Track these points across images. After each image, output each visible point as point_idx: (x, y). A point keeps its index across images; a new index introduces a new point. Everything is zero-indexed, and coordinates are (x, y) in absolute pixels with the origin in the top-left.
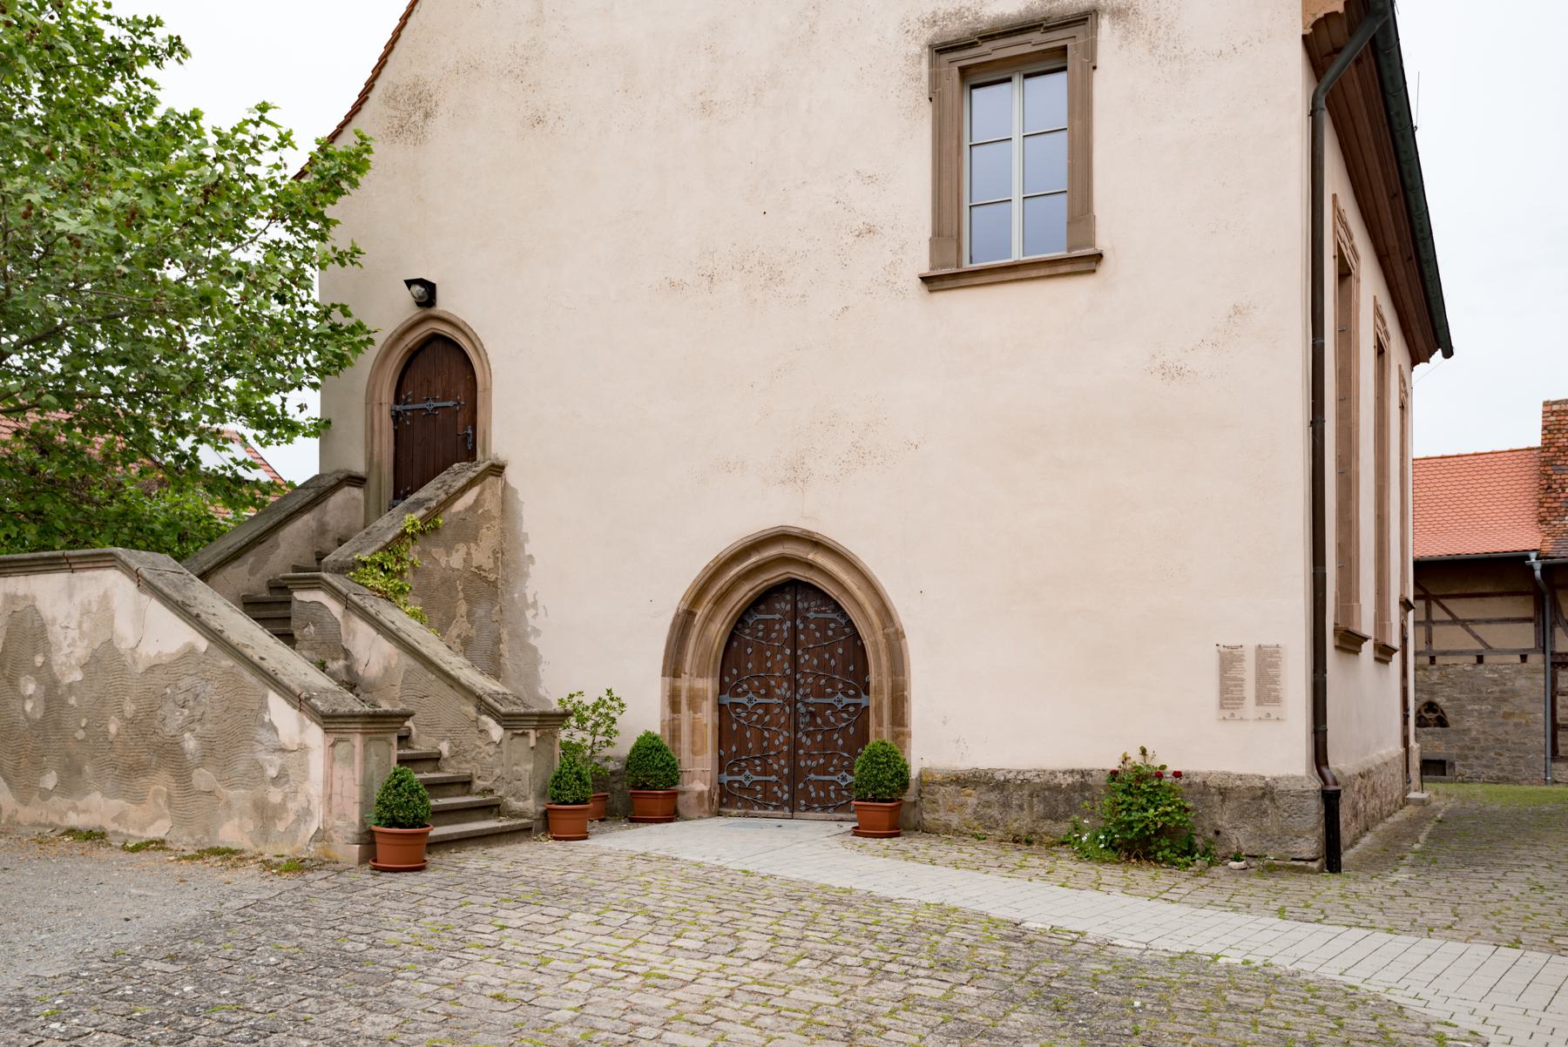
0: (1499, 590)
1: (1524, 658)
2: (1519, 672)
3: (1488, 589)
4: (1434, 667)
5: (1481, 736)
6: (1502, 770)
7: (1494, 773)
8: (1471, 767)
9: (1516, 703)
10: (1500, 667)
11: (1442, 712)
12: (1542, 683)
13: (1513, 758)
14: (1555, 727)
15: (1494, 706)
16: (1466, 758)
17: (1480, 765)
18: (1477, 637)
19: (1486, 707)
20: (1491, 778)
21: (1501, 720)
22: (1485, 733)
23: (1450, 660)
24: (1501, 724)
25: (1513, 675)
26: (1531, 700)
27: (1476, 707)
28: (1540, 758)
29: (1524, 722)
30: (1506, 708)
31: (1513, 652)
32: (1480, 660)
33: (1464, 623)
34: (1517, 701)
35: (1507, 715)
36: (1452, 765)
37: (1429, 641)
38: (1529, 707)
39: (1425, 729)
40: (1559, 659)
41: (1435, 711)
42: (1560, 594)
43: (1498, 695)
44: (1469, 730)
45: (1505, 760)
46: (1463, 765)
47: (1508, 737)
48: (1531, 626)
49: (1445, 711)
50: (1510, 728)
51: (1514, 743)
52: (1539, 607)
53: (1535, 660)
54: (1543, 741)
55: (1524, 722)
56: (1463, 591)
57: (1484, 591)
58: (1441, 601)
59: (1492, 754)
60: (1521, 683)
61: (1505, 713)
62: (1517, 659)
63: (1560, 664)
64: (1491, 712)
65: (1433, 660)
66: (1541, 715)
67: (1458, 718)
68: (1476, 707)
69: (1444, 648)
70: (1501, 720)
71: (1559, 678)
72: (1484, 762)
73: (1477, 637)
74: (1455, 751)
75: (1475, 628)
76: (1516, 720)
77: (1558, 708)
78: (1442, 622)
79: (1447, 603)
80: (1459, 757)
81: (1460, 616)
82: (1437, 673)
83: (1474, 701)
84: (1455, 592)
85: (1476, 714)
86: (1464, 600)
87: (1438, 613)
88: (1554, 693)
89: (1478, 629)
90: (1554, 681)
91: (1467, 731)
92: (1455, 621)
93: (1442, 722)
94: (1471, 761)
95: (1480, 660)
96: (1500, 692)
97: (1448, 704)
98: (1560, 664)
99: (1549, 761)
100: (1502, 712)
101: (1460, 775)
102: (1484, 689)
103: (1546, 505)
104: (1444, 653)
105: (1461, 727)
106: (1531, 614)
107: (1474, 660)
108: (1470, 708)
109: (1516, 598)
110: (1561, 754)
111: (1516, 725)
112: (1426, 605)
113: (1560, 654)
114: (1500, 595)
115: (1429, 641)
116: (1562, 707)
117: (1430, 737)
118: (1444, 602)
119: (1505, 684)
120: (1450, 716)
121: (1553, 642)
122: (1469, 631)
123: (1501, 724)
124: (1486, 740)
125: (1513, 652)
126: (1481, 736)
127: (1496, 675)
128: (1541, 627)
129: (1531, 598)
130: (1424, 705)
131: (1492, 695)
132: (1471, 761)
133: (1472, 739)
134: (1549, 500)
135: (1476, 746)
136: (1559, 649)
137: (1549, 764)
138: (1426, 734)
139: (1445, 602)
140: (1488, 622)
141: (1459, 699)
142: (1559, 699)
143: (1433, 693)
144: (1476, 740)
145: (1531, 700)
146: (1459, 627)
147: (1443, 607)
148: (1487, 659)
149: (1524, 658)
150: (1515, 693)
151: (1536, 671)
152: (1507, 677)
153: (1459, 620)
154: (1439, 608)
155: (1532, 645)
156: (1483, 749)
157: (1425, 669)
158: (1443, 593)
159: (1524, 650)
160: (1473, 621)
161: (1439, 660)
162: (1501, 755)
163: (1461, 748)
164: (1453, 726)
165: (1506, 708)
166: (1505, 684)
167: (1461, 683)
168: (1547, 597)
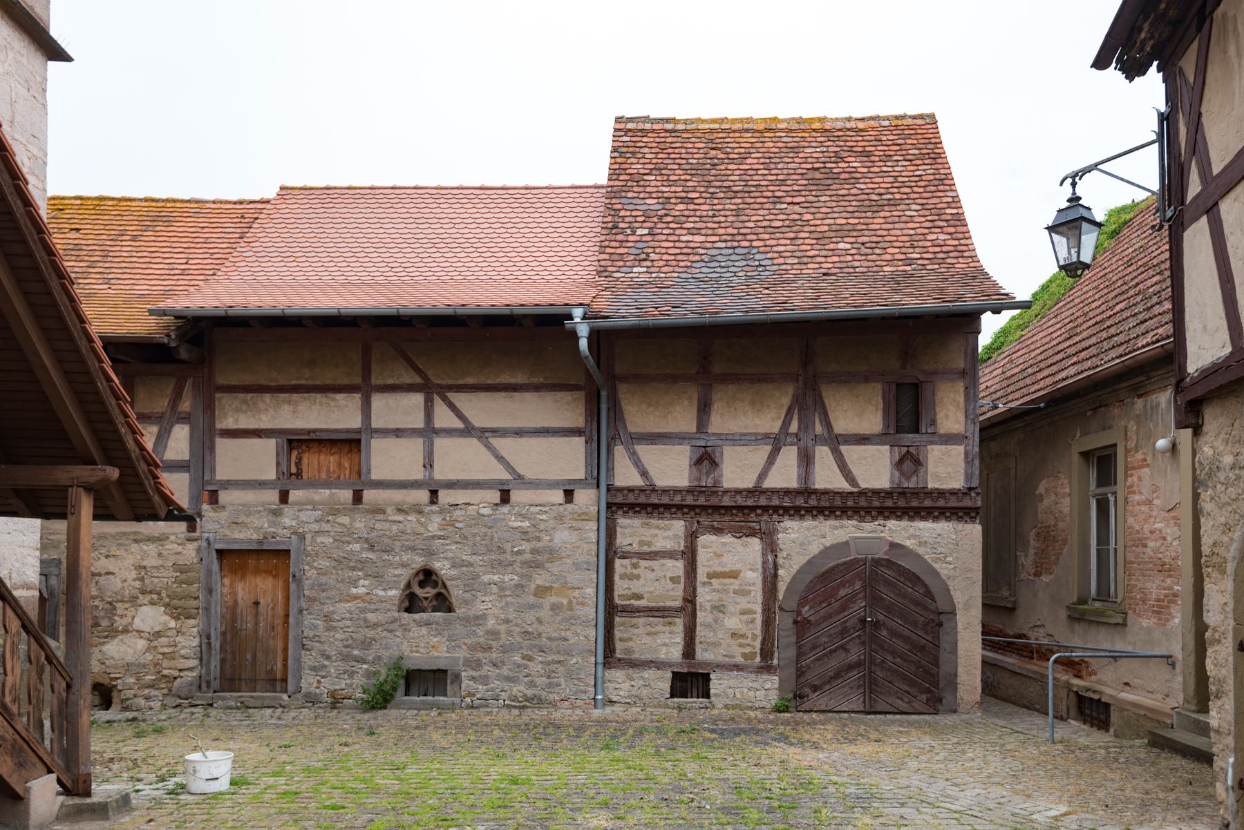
0: (535, 380)
1: (569, 495)
2: (560, 518)
3: (519, 379)
4: (435, 508)
5: (503, 628)
6: (532, 684)
7: (519, 689)
8: (485, 680)
9: (555, 570)
10: (533, 509)
11: (445, 586)
12: (593, 537)
13: (548, 663)
14: (611, 610)
15: (522, 576)
16: (478, 665)
17: (498, 677)
18: (500, 459)
19: (510, 578)
20: (515, 699)
21: (532, 599)
22: (507, 621)
23: (460, 496)
24: (532, 607)
25: (551, 523)
26: (577, 566)
27: (496, 578)
28: (586, 664)
29: (565, 601)
30: (540, 579)
31: (552, 485)
32: (505, 498)
33: (484, 434)
34: (555, 568)
35: (541, 591)
36: (457, 677)
37: (429, 464)
38: (574, 578)
39: (417, 616)
40: (619, 499)
41: (435, 584)
42: (622, 389)
43: (528, 556)
44: (484, 617)
45: (535, 667)
46: (473, 678)
47: (541, 628)
48: (579, 442)
49: (448, 583)
50: (545, 613)
51: (549, 639)
52: (593, 413)
53: (586, 498)
54: (588, 635)
55: (565, 601)
56: (483, 380)
57: (512, 381)
58: (449, 395)
59: (517, 658)
60: (562, 536)
61: (538, 586)
62: (558, 496)
63: (620, 506)
64: (518, 586)
65: (434, 493)
66: (590, 591)
67: (468, 596)
68: (496, 578)
69: (452, 476)
70: (532, 599)
71: (618, 529)
72: (505, 671)
73: (500, 459)
74: (462, 654)
75: (496, 442)
76: (554, 599)
77: (617, 578)
78: (450, 432)
79: (458, 399)
80: (468, 663)
81: (478, 421)
82: (437, 519)
83: (495, 566)
84: (470, 380)
85: (495, 588)
86: (482, 395)
87: (444, 417)
88: (611, 553)
89: (504, 445)
90: (611, 534)
91: (480, 618)
92: (469, 430)
93: (443, 603)
94: (487, 670)
95: (505, 498)
97: (453, 572)
98: (620, 506)
99: (600, 668)
100: (533, 586)
101: (471, 695)
102: (508, 547)
103: (608, 250)
104: (452, 485)
105: (472, 613)
106: (579, 421)
107: (495, 496)
108: (486, 578)
109: (560, 395)
110: (618, 655)
111: (555, 608)
112: (426, 402)
113: (621, 489)
114: (537, 388)
115: (429, 464)
116: (622, 577)
117: (424, 630)
118: (451, 395)
119: (538, 539)
120: (456, 593)
121: (610, 470)
122: (489, 447)
123: (532, 607)
124: (509, 633)
125: (552, 485)
126: (503, 628)
127: (527, 524)
128: (595, 445)
129: (580, 395)
130: (417, 574)
131: (520, 558)
132: (487, 670)
133: (488, 632)
134: (613, 244)
135: (494, 644)
136: (619, 482)
137: (600, 674)
138: (420, 624)
139: (454, 397)
140: (519, 433)
141: (471, 564)
142: (618, 563)
143: (430, 554)
144: (494, 634)
145: (577, 566)
146: (475, 441)
147: (452, 407)
148: (515, 496)
149: (569, 495)
150: (553, 554)
151: (583, 517)
152: (542, 527)
153: (474, 428)
154: (445, 407)
155: (581, 475)
156: (505, 650)
157: (420, 512)
158: (451, 382)
159: (570, 482)
160: (495, 432)
161: (445, 497)
162: (530, 659)
163: (473, 648)
164: (460, 611)
165: (540, 579)
166: (538, 539)
167: (474, 535)
168: (604, 393)
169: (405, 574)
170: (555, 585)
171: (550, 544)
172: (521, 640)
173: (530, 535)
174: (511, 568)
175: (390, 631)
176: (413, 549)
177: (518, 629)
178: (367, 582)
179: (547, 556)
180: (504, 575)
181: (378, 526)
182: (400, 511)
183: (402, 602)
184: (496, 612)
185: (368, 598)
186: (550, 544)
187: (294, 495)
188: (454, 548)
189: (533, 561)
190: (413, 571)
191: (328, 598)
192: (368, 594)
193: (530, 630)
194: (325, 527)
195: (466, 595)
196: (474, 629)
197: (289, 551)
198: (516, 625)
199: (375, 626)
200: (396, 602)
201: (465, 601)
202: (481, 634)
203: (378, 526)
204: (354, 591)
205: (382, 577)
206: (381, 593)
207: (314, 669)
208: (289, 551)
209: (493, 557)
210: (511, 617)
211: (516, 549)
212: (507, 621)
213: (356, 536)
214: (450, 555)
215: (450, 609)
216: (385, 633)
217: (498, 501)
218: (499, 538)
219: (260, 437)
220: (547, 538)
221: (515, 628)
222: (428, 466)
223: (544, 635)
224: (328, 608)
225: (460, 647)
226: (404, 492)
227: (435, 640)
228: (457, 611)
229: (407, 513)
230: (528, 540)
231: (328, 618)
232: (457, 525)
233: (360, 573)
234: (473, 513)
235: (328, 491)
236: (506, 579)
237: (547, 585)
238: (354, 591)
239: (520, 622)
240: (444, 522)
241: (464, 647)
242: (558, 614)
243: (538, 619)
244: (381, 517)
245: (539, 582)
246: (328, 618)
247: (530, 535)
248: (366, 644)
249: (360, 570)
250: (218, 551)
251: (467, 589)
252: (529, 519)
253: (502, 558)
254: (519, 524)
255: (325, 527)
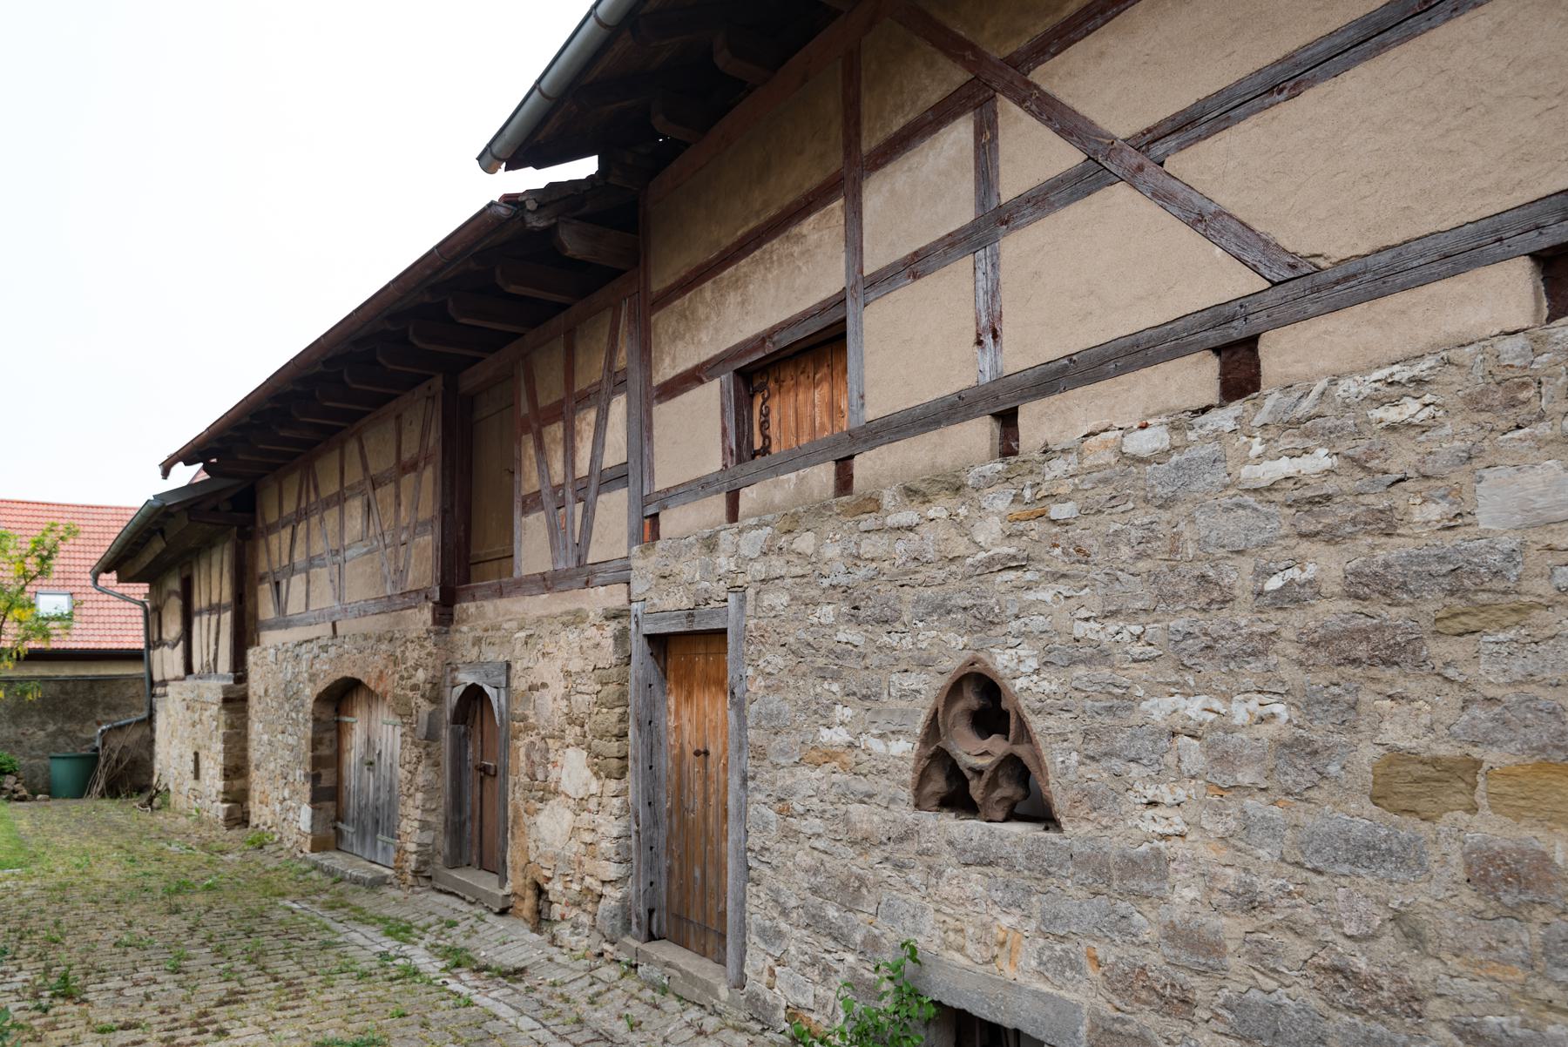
5: (1232, 927)
9: (1489, 676)
11: (1024, 734)
15: (1309, 703)
22: (1250, 902)
24: (1366, 853)
27: (1194, 708)
43: (1332, 612)
49: (1036, 724)
61: (1396, 757)
64: (1297, 748)
68: (1194, 708)
69: (1052, 348)
85: (1193, 754)
96: (1360, 586)
97: (1049, 685)
100: (1368, 754)
102: (1238, 576)
105: (1113, 844)
108: (1159, 709)
117: (975, 881)
119: (1386, 524)
123: (1366, 853)
124: (1262, 955)
126: (1232, 927)
127: (1320, 459)
131: (1295, 621)
133: (1175, 934)
135: (1200, 988)
141: (1102, 655)
152: (1402, 458)
164: (1077, 831)
166: (1386, 524)
167: (1115, 537)
169: (927, 688)
170: (1491, 757)
171: (1450, 540)
172: (1315, 1002)
173: (1338, 513)
174: (1256, 666)
175: (900, 867)
176: (942, 609)
177: (1300, 949)
178: (847, 713)
179: (1434, 603)
180: (1227, 697)
181: (868, 547)
182: (910, 492)
183: (923, 778)
184: (1206, 852)
185: (850, 759)
186: (1450, 540)
187: (749, 497)
188: (1047, 596)
189: (1364, 635)
190: (944, 682)
191: (783, 752)
192: (851, 745)
193: (1361, 964)
194: (778, 565)
195: (1090, 771)
196: (1123, 906)
197: (723, 632)
198: (1292, 927)
199: (863, 843)
200: (909, 777)
201: (1089, 795)
202: (1150, 933)
203: (868, 547)
204: (826, 735)
205: (876, 697)
206: (877, 746)
207: (762, 932)
208: (723, 632)
209: (1180, 623)
210: (1265, 886)
211: (1274, 583)
212: (1250, 902)
213: (826, 583)
214: (1038, 623)
215: (1044, 816)
216: (887, 871)
217: (1211, 394)
218: (1202, 543)
219: (701, 382)
220: (1435, 512)
221: (1288, 938)
222: (988, 339)
223: (1434, 1005)
224: (785, 779)
225: (1075, 966)
226: (933, 436)
227: (1006, 921)
228: (1068, 828)
229: (926, 501)
230: (1331, 537)
231: (782, 803)
232: (1058, 511)
233: (835, 687)
234: (1109, 457)
235: (793, 475)
236: (1240, 712)
237: (1443, 750)
238: (826, 735)
239: (1307, 915)
240: (1017, 509)
241: (1092, 972)
242: (1515, 913)
243: (1397, 918)
244: (868, 522)
245: (1395, 734)
246: (782, 803)
247: (1338, 513)
248: (851, 892)
249: (836, 677)
250: (651, 638)
251: (1092, 748)
252: (1330, 436)
253: (1215, 622)
254: (1285, 466)
255: (778, 565)
